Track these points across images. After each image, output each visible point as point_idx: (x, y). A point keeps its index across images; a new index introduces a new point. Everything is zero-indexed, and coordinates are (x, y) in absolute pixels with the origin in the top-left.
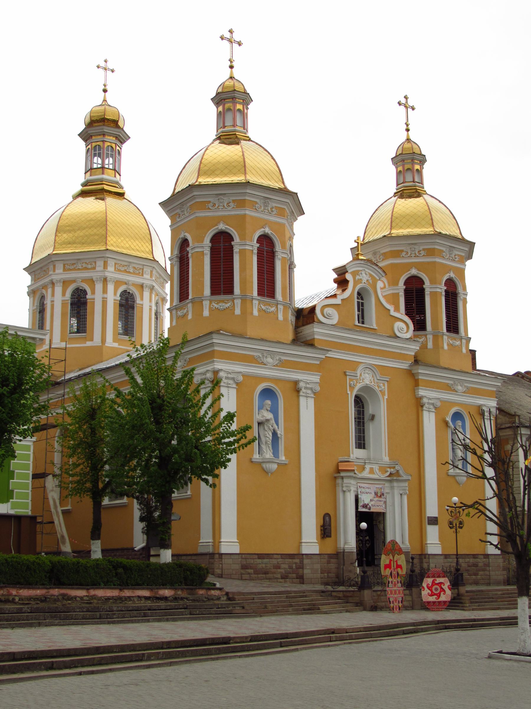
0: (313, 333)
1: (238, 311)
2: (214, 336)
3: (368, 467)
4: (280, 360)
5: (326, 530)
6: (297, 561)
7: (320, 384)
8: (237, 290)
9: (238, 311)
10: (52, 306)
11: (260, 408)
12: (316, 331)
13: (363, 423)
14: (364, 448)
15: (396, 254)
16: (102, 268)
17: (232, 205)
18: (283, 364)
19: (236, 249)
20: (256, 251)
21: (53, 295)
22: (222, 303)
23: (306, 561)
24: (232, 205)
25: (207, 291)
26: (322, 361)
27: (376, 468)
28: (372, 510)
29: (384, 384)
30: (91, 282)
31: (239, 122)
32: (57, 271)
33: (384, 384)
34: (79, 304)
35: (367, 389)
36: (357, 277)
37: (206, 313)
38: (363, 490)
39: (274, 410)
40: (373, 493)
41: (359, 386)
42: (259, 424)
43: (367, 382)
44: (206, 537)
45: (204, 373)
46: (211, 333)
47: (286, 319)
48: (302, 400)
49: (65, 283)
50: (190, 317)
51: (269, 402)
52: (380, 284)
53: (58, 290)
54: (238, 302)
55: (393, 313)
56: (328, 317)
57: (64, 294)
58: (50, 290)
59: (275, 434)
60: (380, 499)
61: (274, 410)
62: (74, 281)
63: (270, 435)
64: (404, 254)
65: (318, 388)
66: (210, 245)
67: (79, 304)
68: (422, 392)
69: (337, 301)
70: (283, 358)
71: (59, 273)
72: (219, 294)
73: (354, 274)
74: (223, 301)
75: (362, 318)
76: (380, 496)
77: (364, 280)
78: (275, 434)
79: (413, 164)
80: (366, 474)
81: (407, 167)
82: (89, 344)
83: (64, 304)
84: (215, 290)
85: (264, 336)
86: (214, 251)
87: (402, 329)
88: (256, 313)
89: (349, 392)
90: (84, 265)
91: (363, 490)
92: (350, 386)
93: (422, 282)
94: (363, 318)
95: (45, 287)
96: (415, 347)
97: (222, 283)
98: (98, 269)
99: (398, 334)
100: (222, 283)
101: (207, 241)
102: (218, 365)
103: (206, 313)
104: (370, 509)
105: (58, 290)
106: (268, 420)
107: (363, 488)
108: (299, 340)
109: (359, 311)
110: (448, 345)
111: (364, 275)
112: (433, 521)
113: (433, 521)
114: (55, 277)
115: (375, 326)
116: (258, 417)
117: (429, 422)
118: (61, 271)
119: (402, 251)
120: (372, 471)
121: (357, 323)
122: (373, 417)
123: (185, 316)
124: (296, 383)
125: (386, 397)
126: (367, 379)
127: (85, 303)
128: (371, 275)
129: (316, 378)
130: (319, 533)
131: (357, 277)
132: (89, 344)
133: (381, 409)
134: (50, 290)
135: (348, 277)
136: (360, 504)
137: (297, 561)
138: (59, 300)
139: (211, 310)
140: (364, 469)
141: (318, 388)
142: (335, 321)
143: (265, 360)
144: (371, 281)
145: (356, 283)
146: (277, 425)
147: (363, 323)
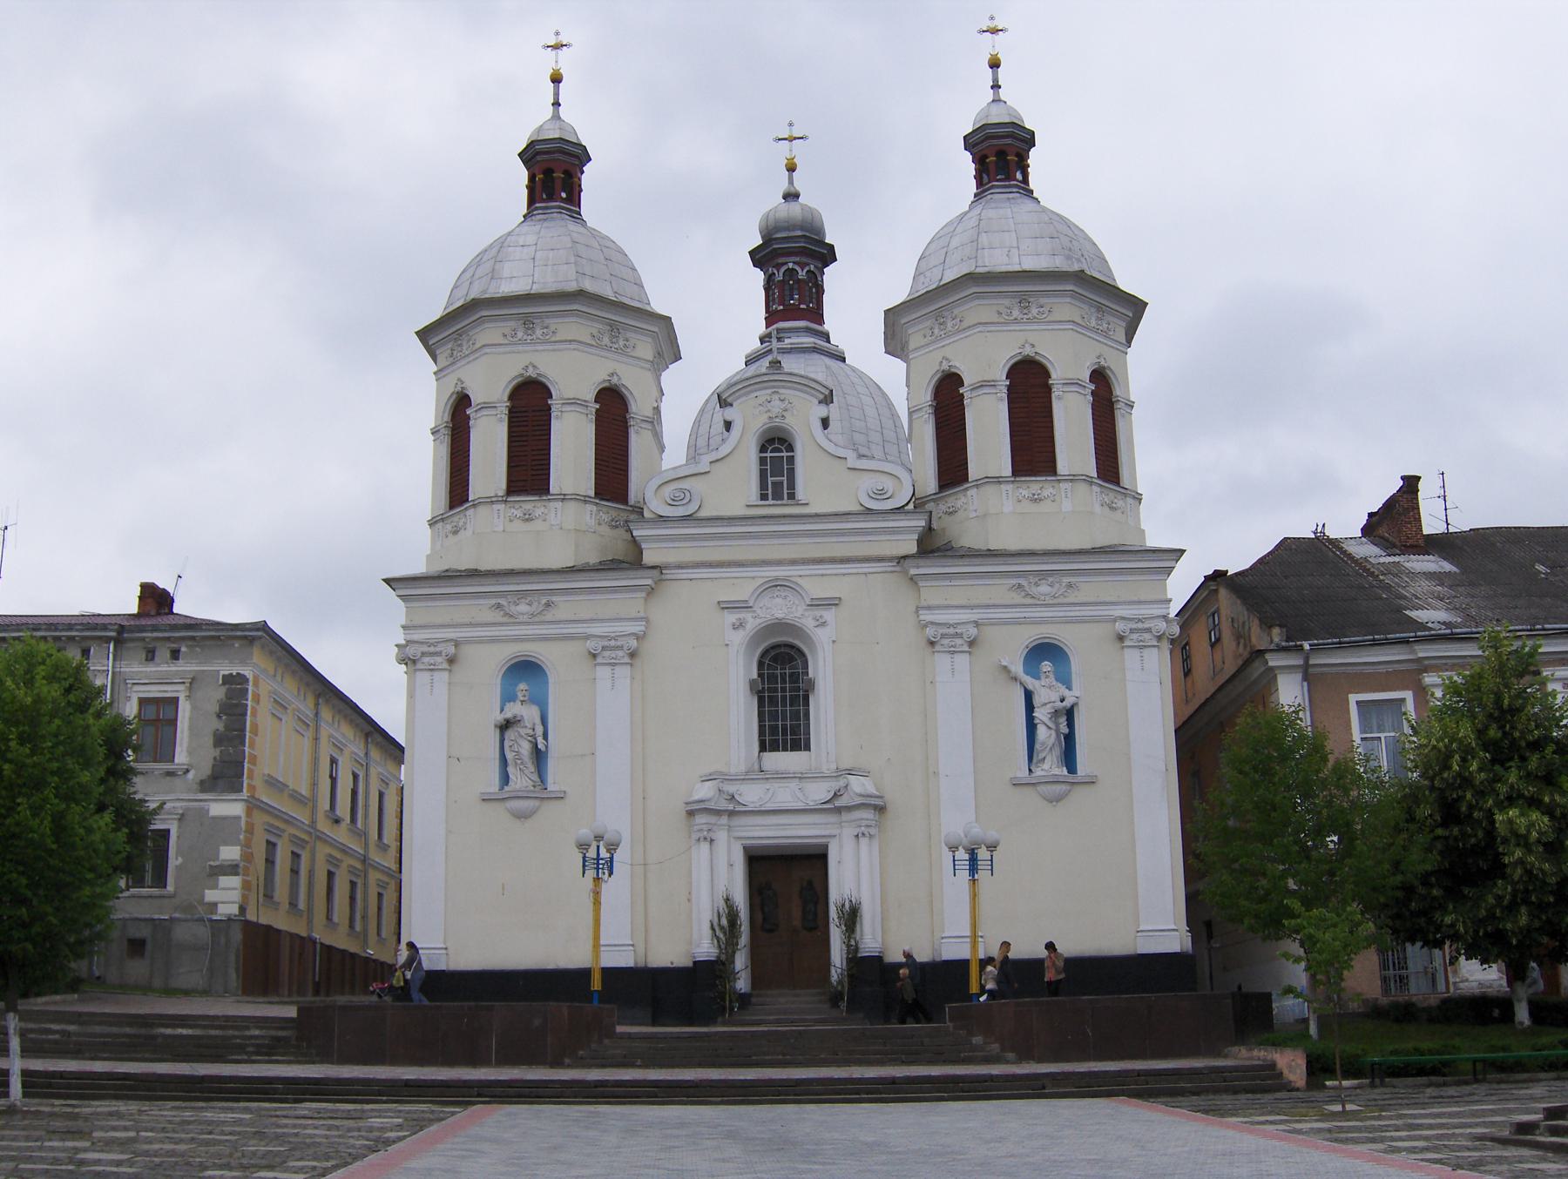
11: (508, 697)
35: (780, 626)
43: (780, 615)
51: (522, 686)
63: (525, 748)
94: (792, 485)
147: (792, 496)
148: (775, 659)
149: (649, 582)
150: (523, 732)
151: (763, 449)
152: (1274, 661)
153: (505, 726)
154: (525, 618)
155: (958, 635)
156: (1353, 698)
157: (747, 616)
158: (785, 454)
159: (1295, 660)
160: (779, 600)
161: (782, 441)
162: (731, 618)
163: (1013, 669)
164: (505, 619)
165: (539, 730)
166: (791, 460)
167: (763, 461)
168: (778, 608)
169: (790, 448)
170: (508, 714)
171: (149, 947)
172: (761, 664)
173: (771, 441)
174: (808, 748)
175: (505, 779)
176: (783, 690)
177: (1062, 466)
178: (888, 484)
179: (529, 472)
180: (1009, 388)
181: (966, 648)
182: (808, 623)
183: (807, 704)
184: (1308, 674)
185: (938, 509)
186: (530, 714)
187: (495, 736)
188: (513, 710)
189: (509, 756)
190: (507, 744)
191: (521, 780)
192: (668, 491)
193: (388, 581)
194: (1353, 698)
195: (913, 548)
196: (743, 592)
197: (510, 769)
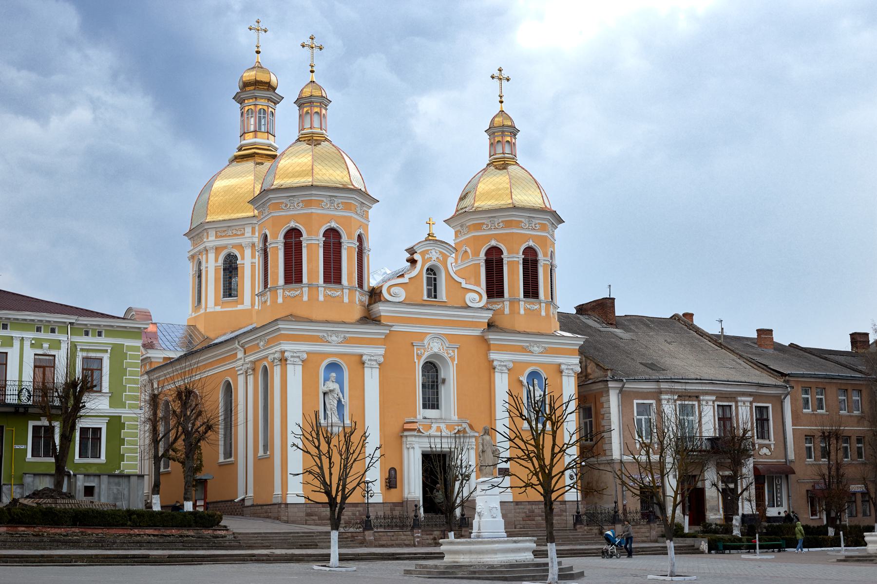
0: (379, 311)
1: (305, 298)
2: (279, 322)
3: (434, 426)
4: (345, 338)
5: (392, 481)
7: (384, 356)
8: (305, 280)
9: (305, 298)
10: (207, 271)
11: (326, 380)
12: (381, 309)
13: (437, 386)
14: (438, 408)
15: (478, 227)
16: (250, 235)
17: (301, 204)
18: (347, 341)
19: (304, 244)
20: (322, 245)
21: (207, 262)
22: (293, 291)
24: (301, 204)
25: (281, 281)
26: (387, 336)
27: (443, 426)
29: (453, 351)
30: (240, 247)
31: (316, 124)
32: (210, 239)
33: (453, 351)
34: (231, 268)
35: (435, 355)
36: (427, 256)
37: (280, 300)
39: (340, 381)
41: (427, 354)
42: (325, 394)
43: (436, 350)
44: (278, 491)
45: (274, 353)
46: (276, 320)
47: (351, 301)
48: (367, 371)
49: (218, 249)
50: (268, 303)
51: (334, 374)
52: (451, 260)
53: (212, 256)
54: (305, 290)
55: (464, 285)
56: (395, 295)
57: (216, 261)
58: (204, 256)
59: (339, 401)
61: (340, 381)
62: (225, 247)
64: (484, 227)
65: (382, 360)
66: (283, 241)
67: (231, 268)
68: (493, 356)
69: (405, 280)
70: (347, 335)
71: (211, 240)
72: (291, 283)
73: (423, 254)
74: (293, 289)
75: (433, 292)
77: (434, 258)
78: (339, 401)
79: (503, 136)
80: (433, 432)
81: (497, 139)
82: (240, 307)
83: (217, 269)
84: (288, 280)
85: (329, 319)
86: (287, 246)
87: (474, 300)
88: (321, 298)
89: (416, 360)
90: (234, 232)
92: (417, 355)
93: (501, 252)
94: (435, 291)
95: (200, 253)
96: (489, 315)
97: (293, 274)
98: (247, 235)
99: (470, 304)
100: (293, 274)
101: (281, 238)
102: (285, 346)
103: (280, 300)
105: (212, 256)
106: (331, 391)
108: (369, 318)
109: (429, 284)
110: (525, 310)
111: (434, 253)
114: (207, 244)
115: (445, 299)
116: (322, 388)
117: (502, 384)
118: (213, 238)
119: (483, 224)
120: (439, 429)
121: (425, 298)
122: (444, 381)
123: (266, 302)
124: (361, 356)
125: (456, 362)
126: (436, 347)
127: (236, 268)
128: (441, 252)
129: (381, 351)
130: (384, 484)
131: (427, 256)
132: (240, 307)
133: (450, 374)
134: (204, 256)
135: (416, 257)
138: (213, 266)
139: (284, 297)
140: (431, 427)
141: (382, 360)
142: (401, 299)
143: (330, 339)
145: (424, 262)
146: (342, 392)
147: (435, 297)
152: (611, 384)
156: (635, 401)
159: (619, 385)
161: (432, 270)
166: (435, 279)
169: (435, 274)
171: (96, 490)
178: (476, 296)
184: (621, 391)
186: (336, 386)
192: (393, 290)
194: (635, 401)
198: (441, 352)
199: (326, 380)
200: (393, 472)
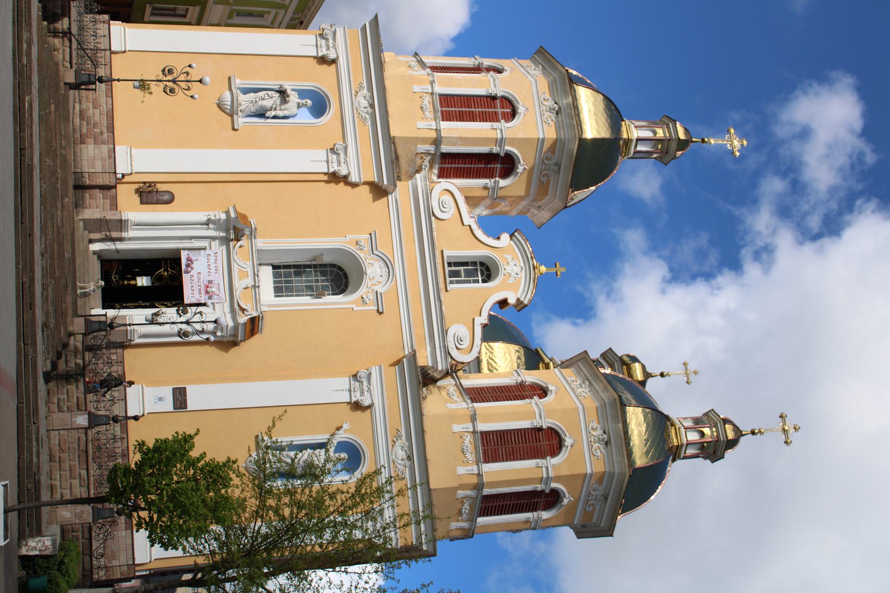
5: (150, 194)
6: (105, 135)
11: (302, 94)
23: (105, 148)
27: (249, 282)
28: (184, 275)
35: (361, 274)
36: (509, 258)
38: (212, 258)
40: (210, 278)
43: (369, 271)
56: (442, 205)
60: (203, 292)
63: (268, 103)
76: (207, 292)
91: (212, 258)
94: (458, 282)
104: (187, 272)
107: (216, 260)
112: (180, 398)
113: (180, 398)
116: (287, 86)
136: (192, 255)
137: (105, 135)
144: (511, 281)
147: (451, 282)
148: (337, 274)
149: (385, 183)
150: (278, 102)
151: (482, 264)
153: (282, 93)
154: (356, 104)
155: (362, 394)
157: (367, 248)
158: (480, 278)
160: (379, 271)
162: (364, 238)
163: (341, 432)
164: (354, 93)
165: (280, 113)
167: (474, 264)
168: (374, 270)
169: (484, 281)
170: (289, 92)
172: (333, 266)
173: (488, 269)
174: (276, 296)
175: (246, 91)
176: (317, 281)
177: (487, 468)
178: (466, 344)
179: (455, 107)
180: (540, 429)
181: (354, 399)
182: (362, 291)
183: (307, 295)
185: (448, 382)
187: (275, 84)
188: (294, 98)
189: (261, 94)
190: (269, 92)
191: (245, 101)
192: (447, 198)
193: (376, 17)
195: (421, 362)
196: (382, 248)
197: (252, 95)
198: (366, 282)
199: (302, 94)
200: (166, 197)
